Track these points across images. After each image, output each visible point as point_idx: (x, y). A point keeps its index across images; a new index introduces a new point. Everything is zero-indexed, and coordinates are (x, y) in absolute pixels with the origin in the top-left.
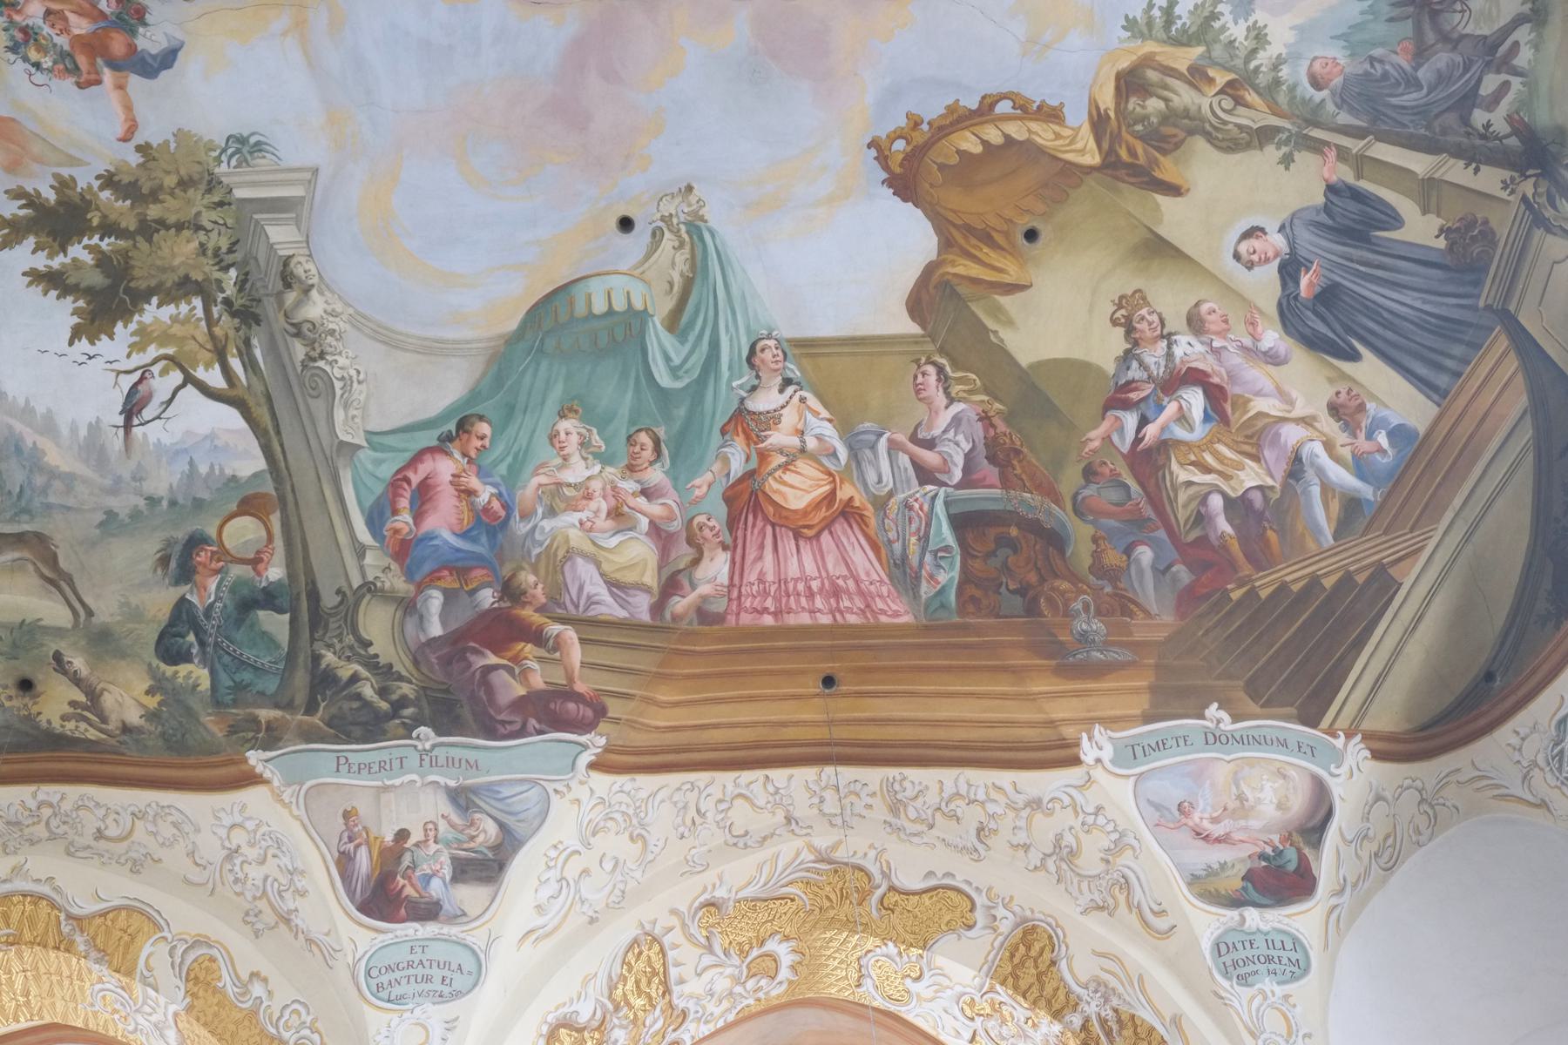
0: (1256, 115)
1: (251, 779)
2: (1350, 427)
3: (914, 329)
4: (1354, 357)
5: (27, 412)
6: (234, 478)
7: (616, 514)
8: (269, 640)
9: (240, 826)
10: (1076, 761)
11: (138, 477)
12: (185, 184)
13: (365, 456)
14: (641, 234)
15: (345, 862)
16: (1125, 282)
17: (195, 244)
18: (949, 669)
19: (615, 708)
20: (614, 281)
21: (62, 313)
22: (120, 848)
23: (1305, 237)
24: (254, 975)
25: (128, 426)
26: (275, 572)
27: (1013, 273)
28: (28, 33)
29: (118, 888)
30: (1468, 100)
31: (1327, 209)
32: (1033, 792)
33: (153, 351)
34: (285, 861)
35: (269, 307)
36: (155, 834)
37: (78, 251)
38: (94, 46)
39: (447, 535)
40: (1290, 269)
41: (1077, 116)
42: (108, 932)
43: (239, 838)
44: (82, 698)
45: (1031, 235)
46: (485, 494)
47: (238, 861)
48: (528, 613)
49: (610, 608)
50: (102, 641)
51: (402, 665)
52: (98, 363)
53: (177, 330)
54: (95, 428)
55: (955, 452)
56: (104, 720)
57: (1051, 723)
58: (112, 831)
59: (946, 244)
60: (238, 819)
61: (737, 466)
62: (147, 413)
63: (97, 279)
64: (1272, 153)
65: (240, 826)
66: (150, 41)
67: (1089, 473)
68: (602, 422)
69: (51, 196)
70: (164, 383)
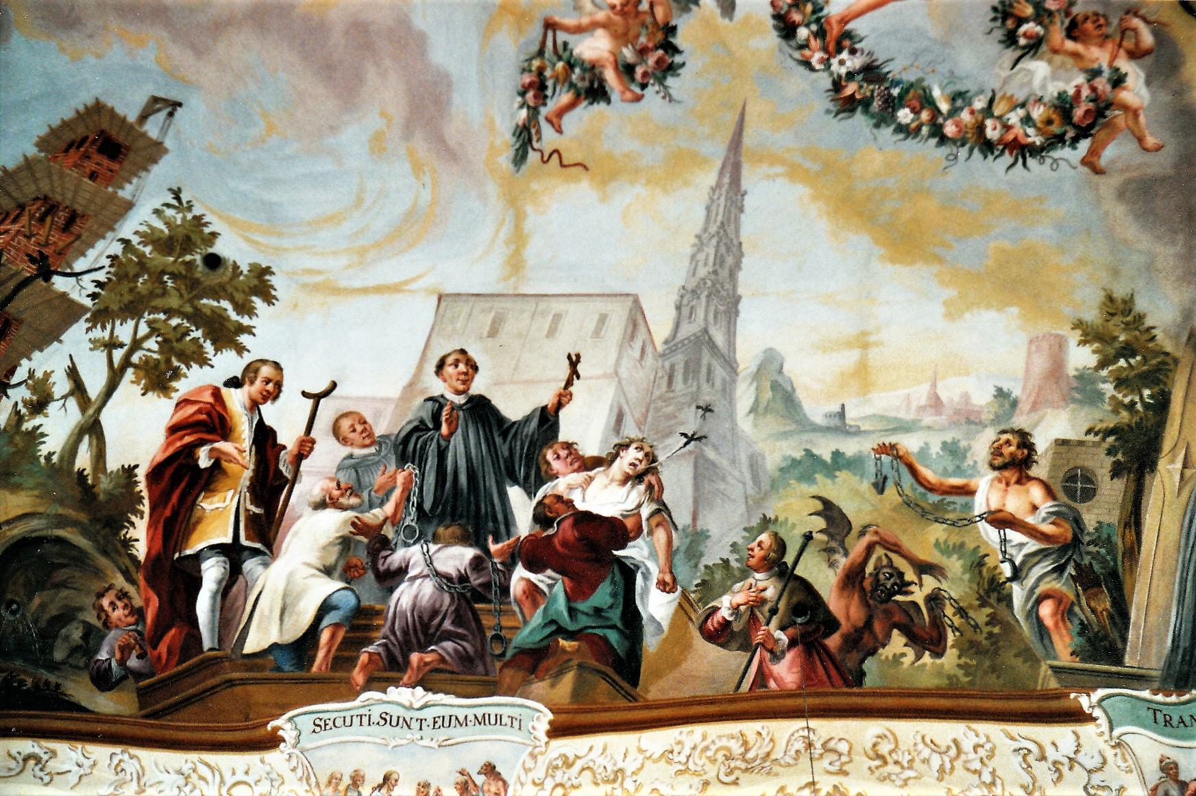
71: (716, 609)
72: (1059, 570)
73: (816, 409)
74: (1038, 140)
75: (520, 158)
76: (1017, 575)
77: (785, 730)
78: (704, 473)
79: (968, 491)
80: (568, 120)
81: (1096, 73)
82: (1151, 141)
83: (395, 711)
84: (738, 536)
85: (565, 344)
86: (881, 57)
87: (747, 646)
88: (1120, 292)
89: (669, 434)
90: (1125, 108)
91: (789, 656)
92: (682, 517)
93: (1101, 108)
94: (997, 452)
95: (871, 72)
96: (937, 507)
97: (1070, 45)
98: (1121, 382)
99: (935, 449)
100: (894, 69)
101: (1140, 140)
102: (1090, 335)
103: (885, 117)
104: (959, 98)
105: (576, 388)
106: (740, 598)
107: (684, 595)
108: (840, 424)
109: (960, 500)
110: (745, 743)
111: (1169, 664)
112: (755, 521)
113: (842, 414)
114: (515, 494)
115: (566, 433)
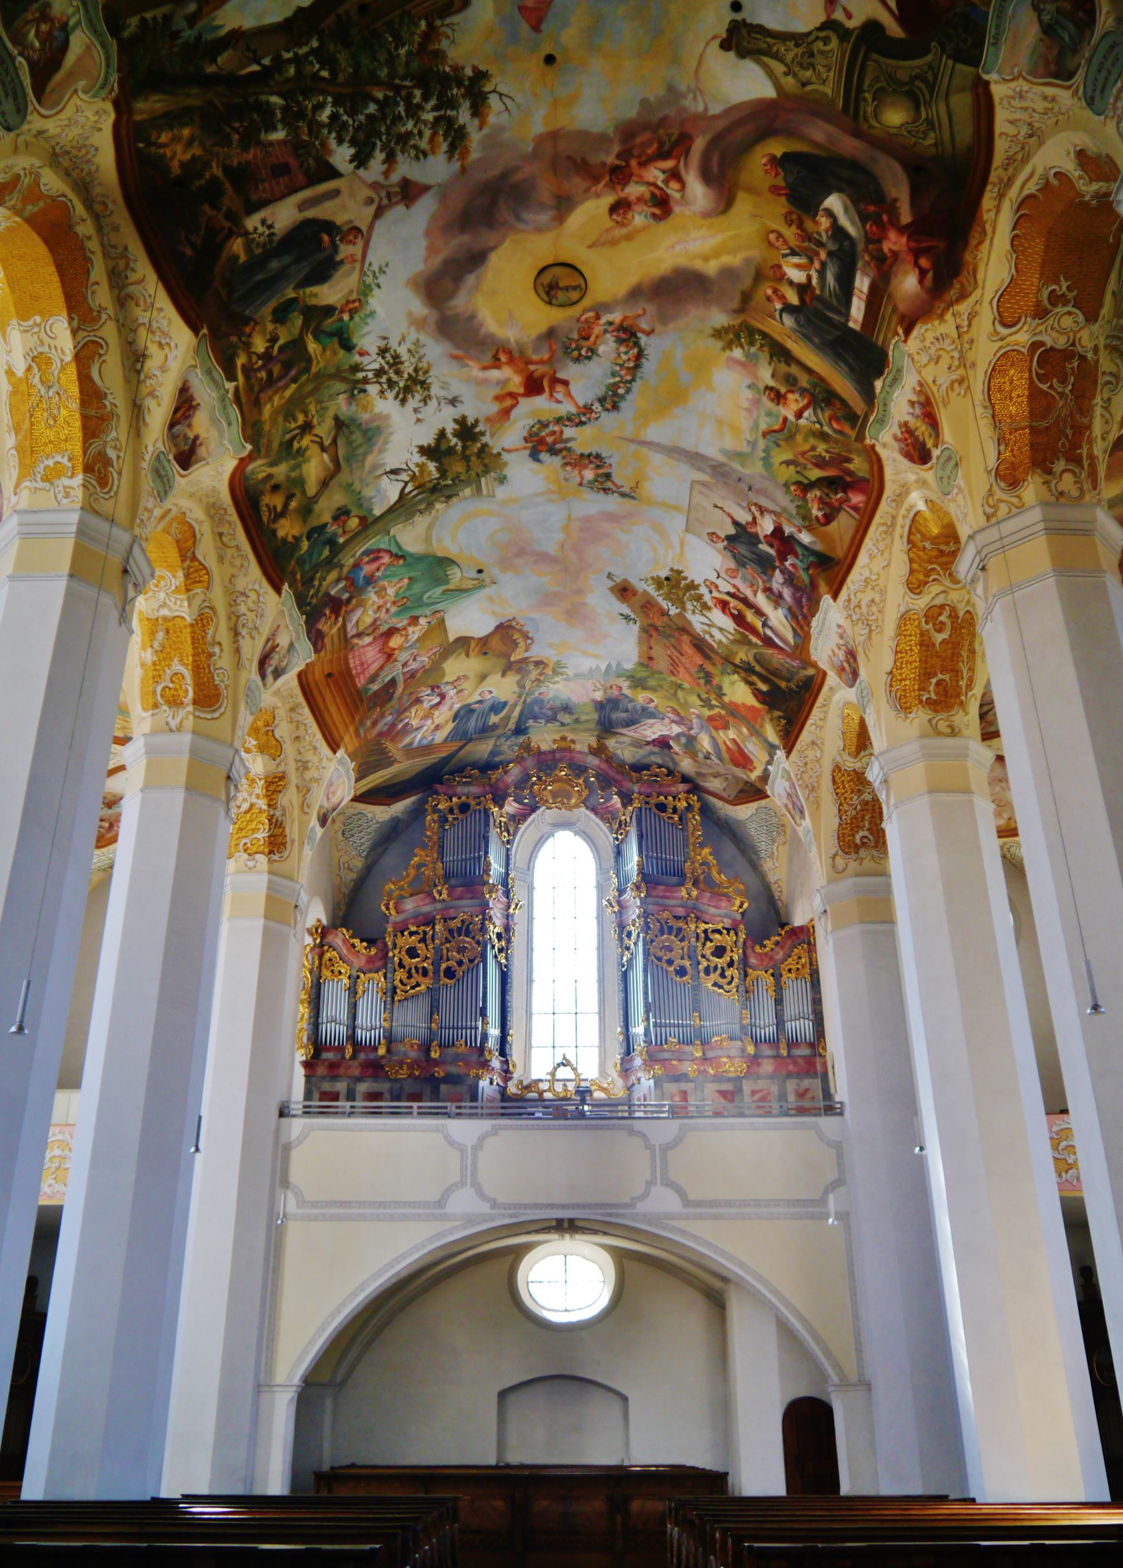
0: (528, 684)
1: (278, 591)
2: (433, 731)
3: (452, 637)
4: (454, 721)
5: (386, 442)
6: (372, 510)
7: (379, 608)
8: (320, 554)
9: (259, 595)
10: (335, 752)
11: (367, 485)
12: (486, 466)
13: (386, 538)
14: (479, 576)
15: (268, 640)
16: (471, 674)
17: (460, 470)
18: (347, 703)
19: (322, 654)
20: (459, 574)
21: (428, 439)
22: (220, 545)
23: (490, 702)
24: (219, 644)
25: (386, 473)
26: (341, 540)
27: (471, 653)
28: (546, 425)
29: (211, 562)
30: (535, 718)
31: (499, 703)
32: (318, 746)
33: (416, 470)
34: (258, 623)
35: (438, 494)
36: (233, 557)
37: (454, 441)
38: (541, 441)
39: (363, 573)
40: (480, 702)
41: (527, 655)
42: (196, 571)
43: (253, 595)
44: (279, 509)
45: (485, 654)
46: (377, 574)
47: (243, 598)
48: (344, 609)
49: (349, 626)
50: (306, 511)
51: (320, 594)
52: (409, 456)
53: (426, 474)
54: (383, 464)
55: (414, 666)
56: (275, 521)
57: (342, 739)
58: (225, 539)
59: (480, 639)
60: (261, 592)
61: (399, 626)
62: (393, 477)
63: (444, 447)
64: (517, 689)
65: (259, 595)
66: (544, 456)
67: (411, 694)
68: (409, 587)
69: (477, 430)
70: (405, 477)
71: (817, 518)
72: (822, 410)
73: (746, 449)
74: (636, 350)
75: (633, 498)
76: (821, 425)
77: (884, 507)
78: (762, 492)
79: (785, 419)
80: (619, 483)
81: (606, 331)
82: (640, 312)
83: (817, 630)
84: (788, 498)
85: (710, 507)
86: (594, 397)
87: (839, 510)
88: (711, 332)
89: (747, 496)
90: (623, 321)
91: (851, 495)
92: (778, 510)
93: (621, 328)
94: (773, 400)
95: (602, 400)
96: (790, 431)
97: (592, 339)
98: (752, 343)
99: (767, 419)
100: (600, 393)
101: (639, 316)
102: (729, 346)
103: (622, 397)
104: (614, 374)
105: (727, 510)
106: (816, 506)
107: (805, 527)
108: (753, 444)
109: (788, 424)
110: (883, 524)
111: (864, 400)
112: (784, 489)
113: (749, 442)
114: (760, 546)
115: (743, 522)
